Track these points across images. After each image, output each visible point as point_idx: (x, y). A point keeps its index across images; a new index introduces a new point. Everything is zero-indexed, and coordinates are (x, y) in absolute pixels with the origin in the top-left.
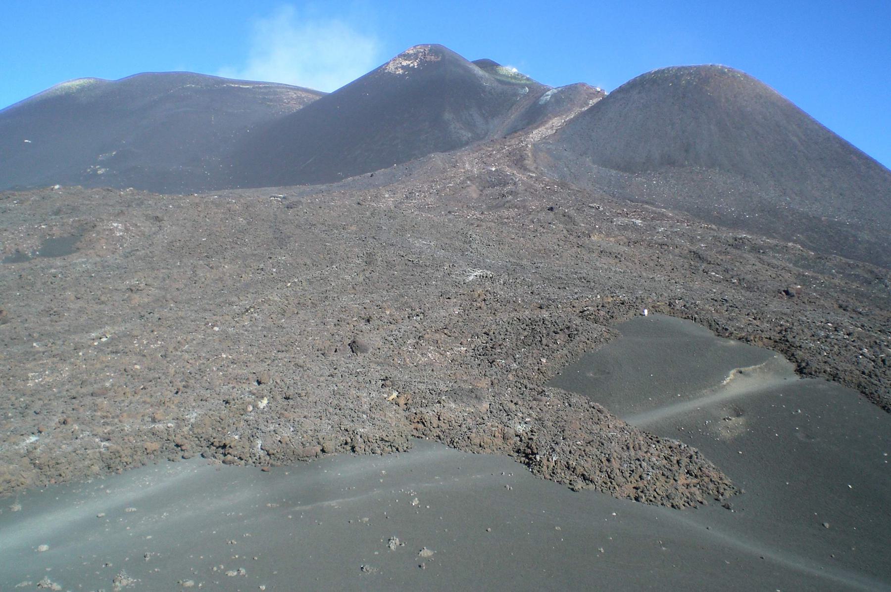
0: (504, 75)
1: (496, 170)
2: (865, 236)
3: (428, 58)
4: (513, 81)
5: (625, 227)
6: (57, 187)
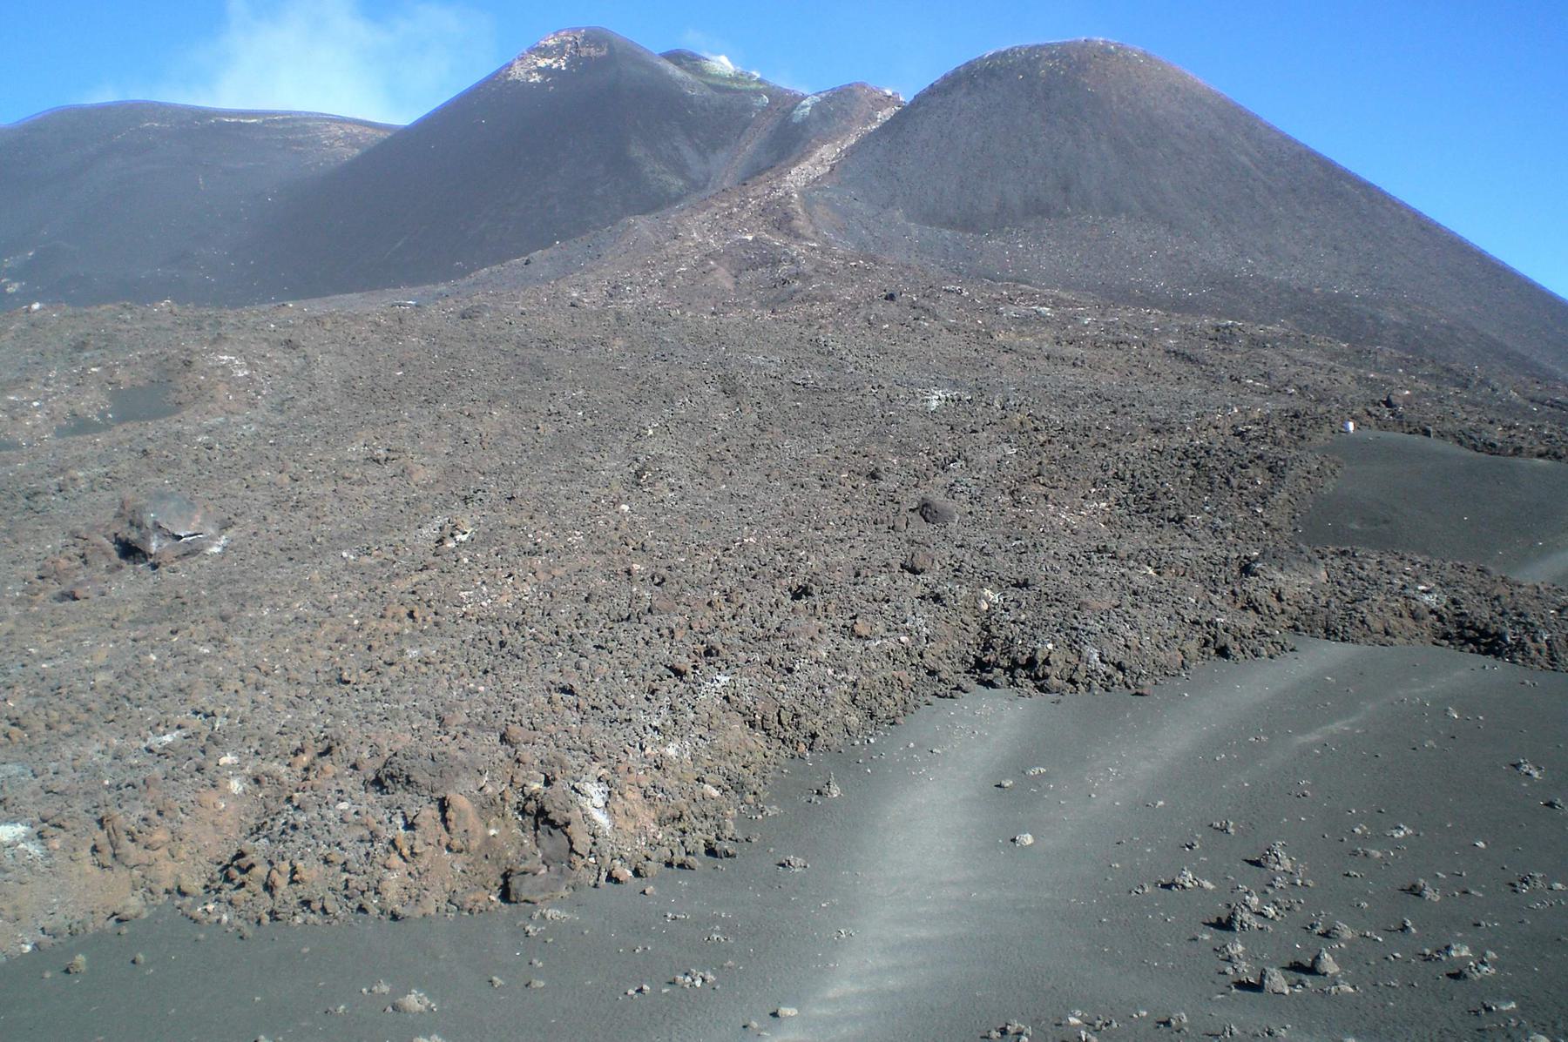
0: (716, 77)
1: (755, 240)
3: (584, 52)
4: (735, 85)
5: (1025, 320)
6: (36, 306)
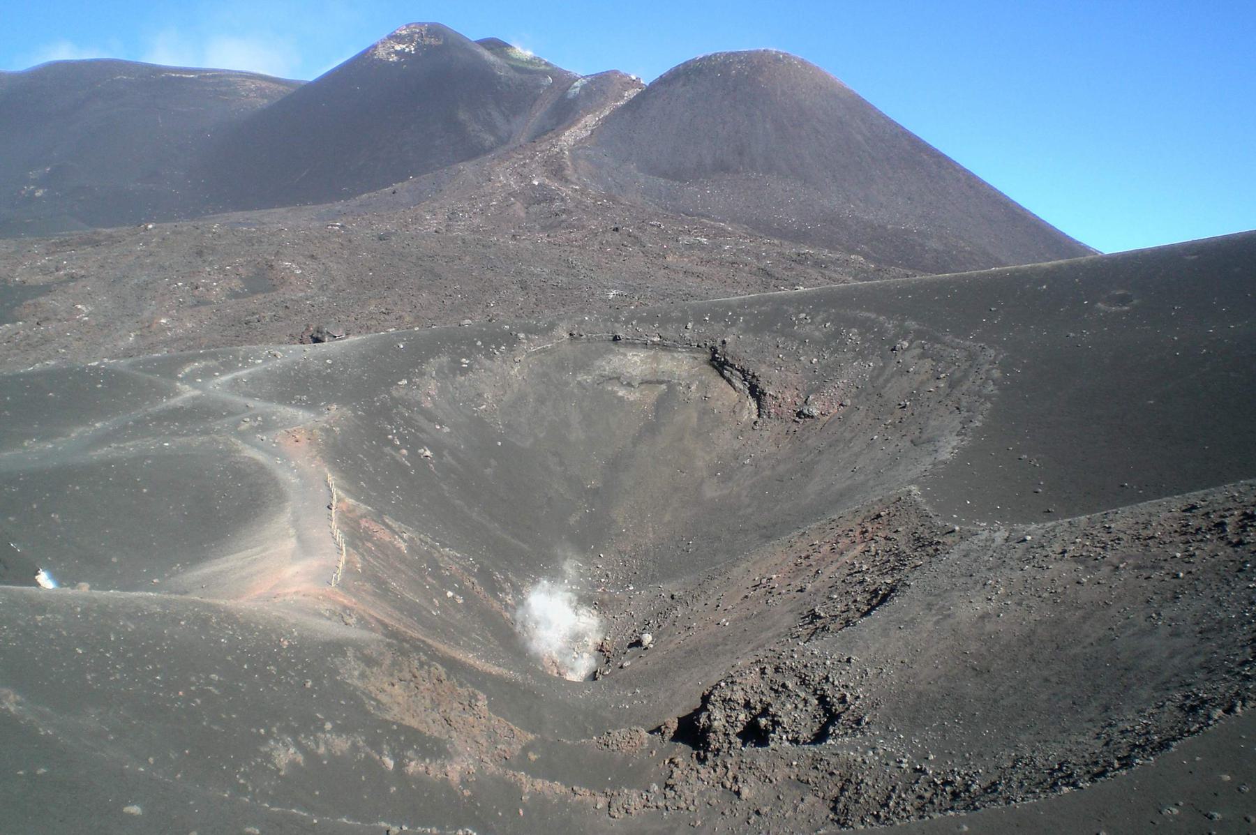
2: (933, 244)
5: (691, 247)
